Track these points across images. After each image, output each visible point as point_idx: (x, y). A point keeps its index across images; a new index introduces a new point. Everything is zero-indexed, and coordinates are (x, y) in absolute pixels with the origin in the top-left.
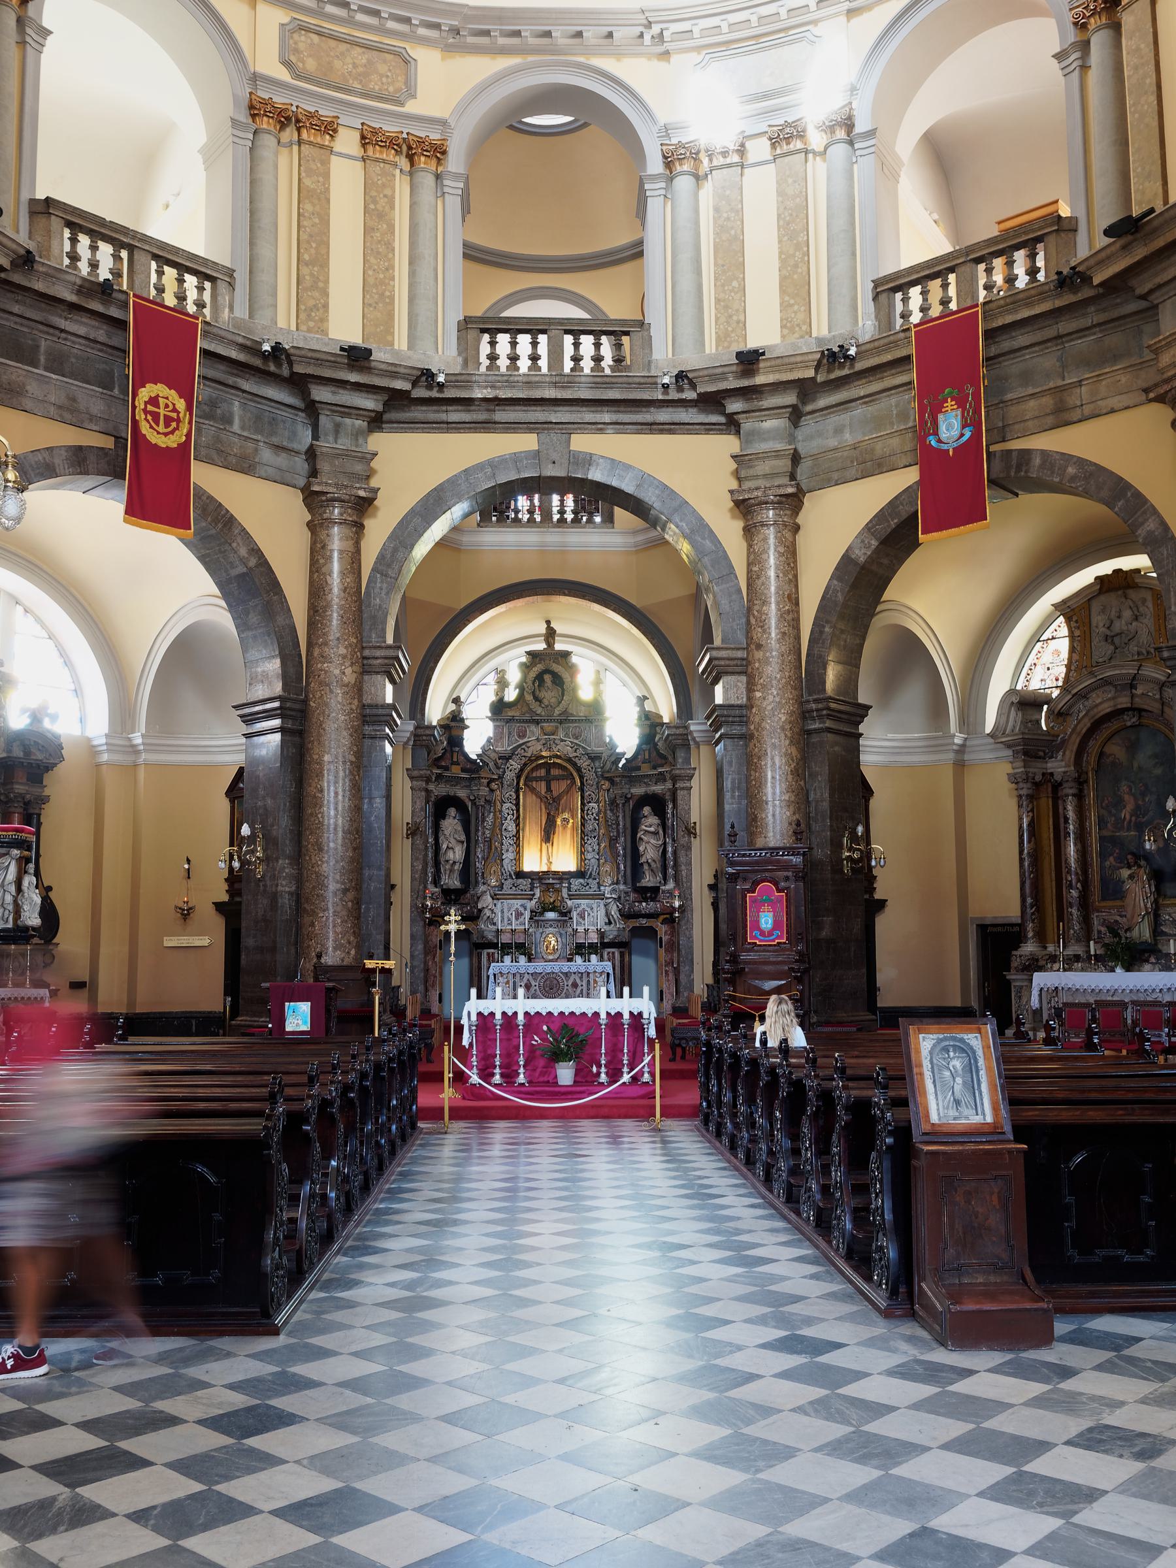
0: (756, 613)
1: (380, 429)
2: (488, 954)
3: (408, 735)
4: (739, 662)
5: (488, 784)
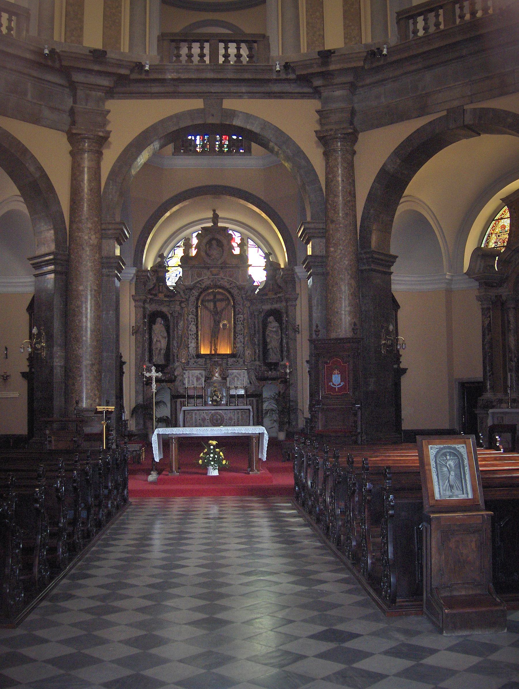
0: (330, 202)
1: (112, 97)
2: (181, 401)
3: (132, 275)
4: (321, 231)
5: (180, 303)
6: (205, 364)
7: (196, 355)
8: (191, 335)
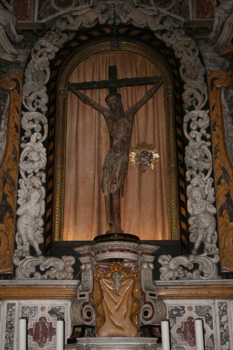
6: (77, 273)
7: (40, 245)
8: (27, 174)
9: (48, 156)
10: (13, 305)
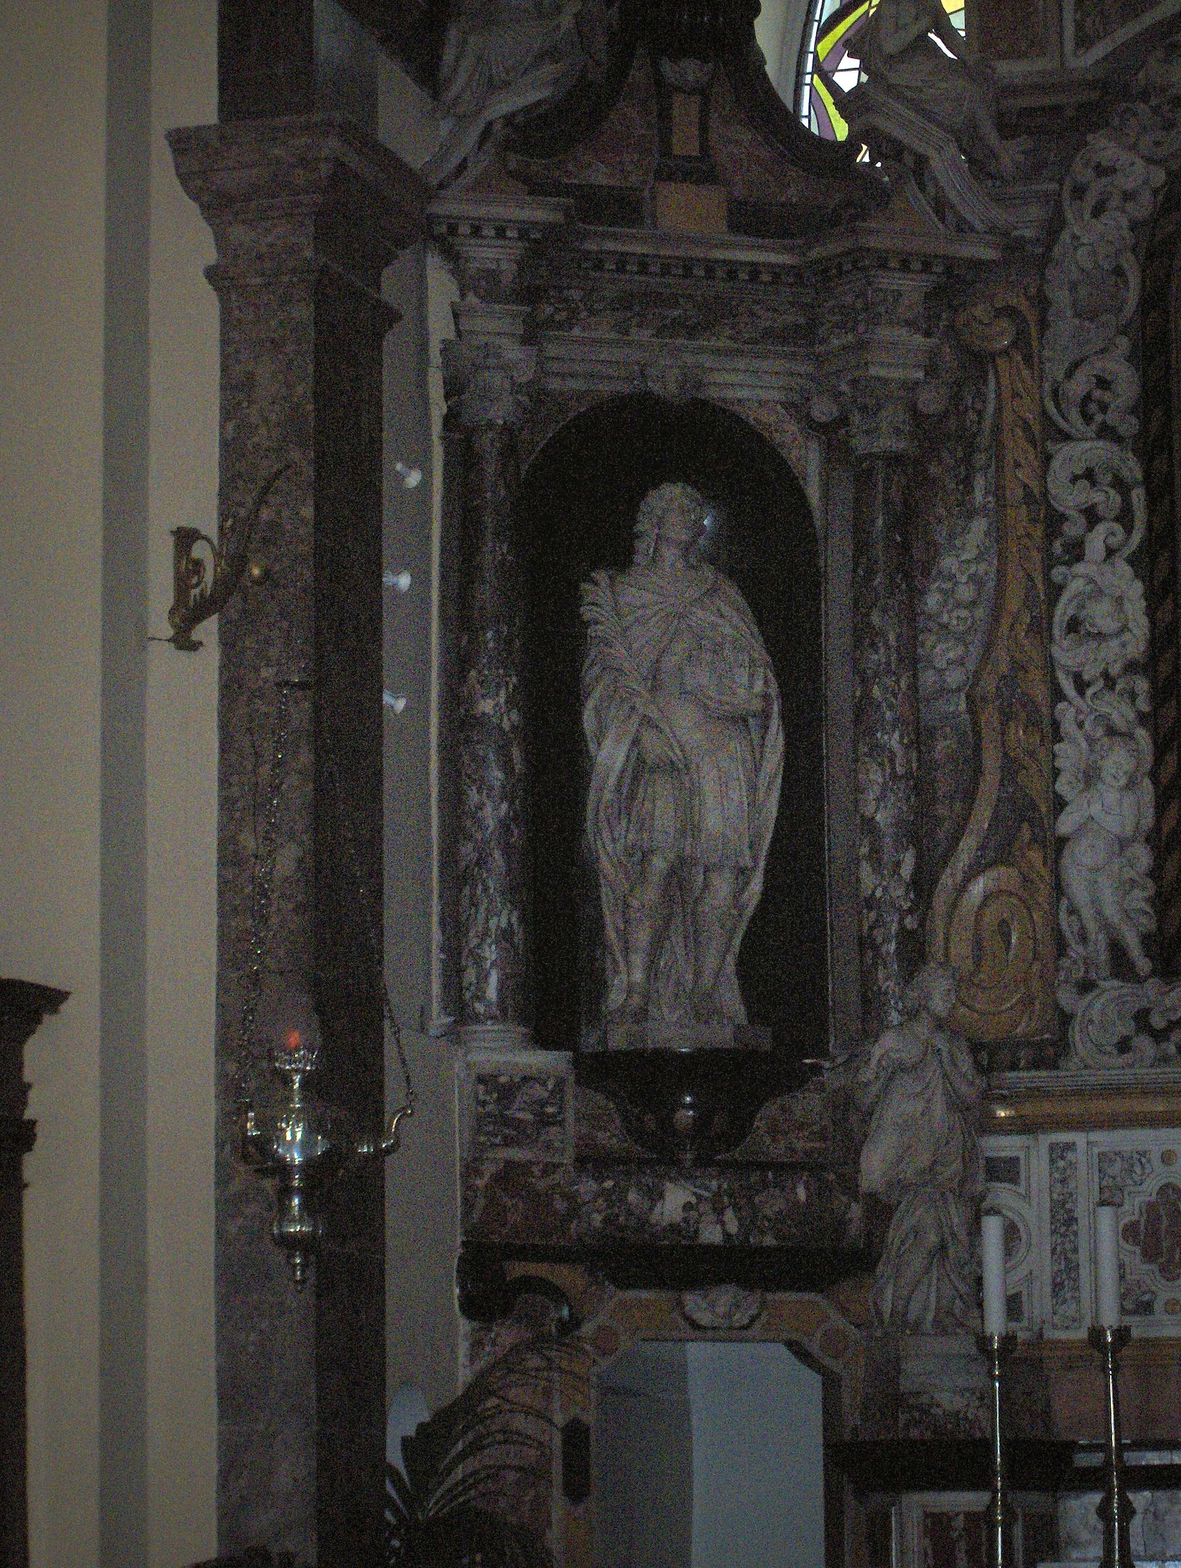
2: (937, 1524)
7: (1146, 940)
9: (1151, 612)
10: (1070, 1146)
